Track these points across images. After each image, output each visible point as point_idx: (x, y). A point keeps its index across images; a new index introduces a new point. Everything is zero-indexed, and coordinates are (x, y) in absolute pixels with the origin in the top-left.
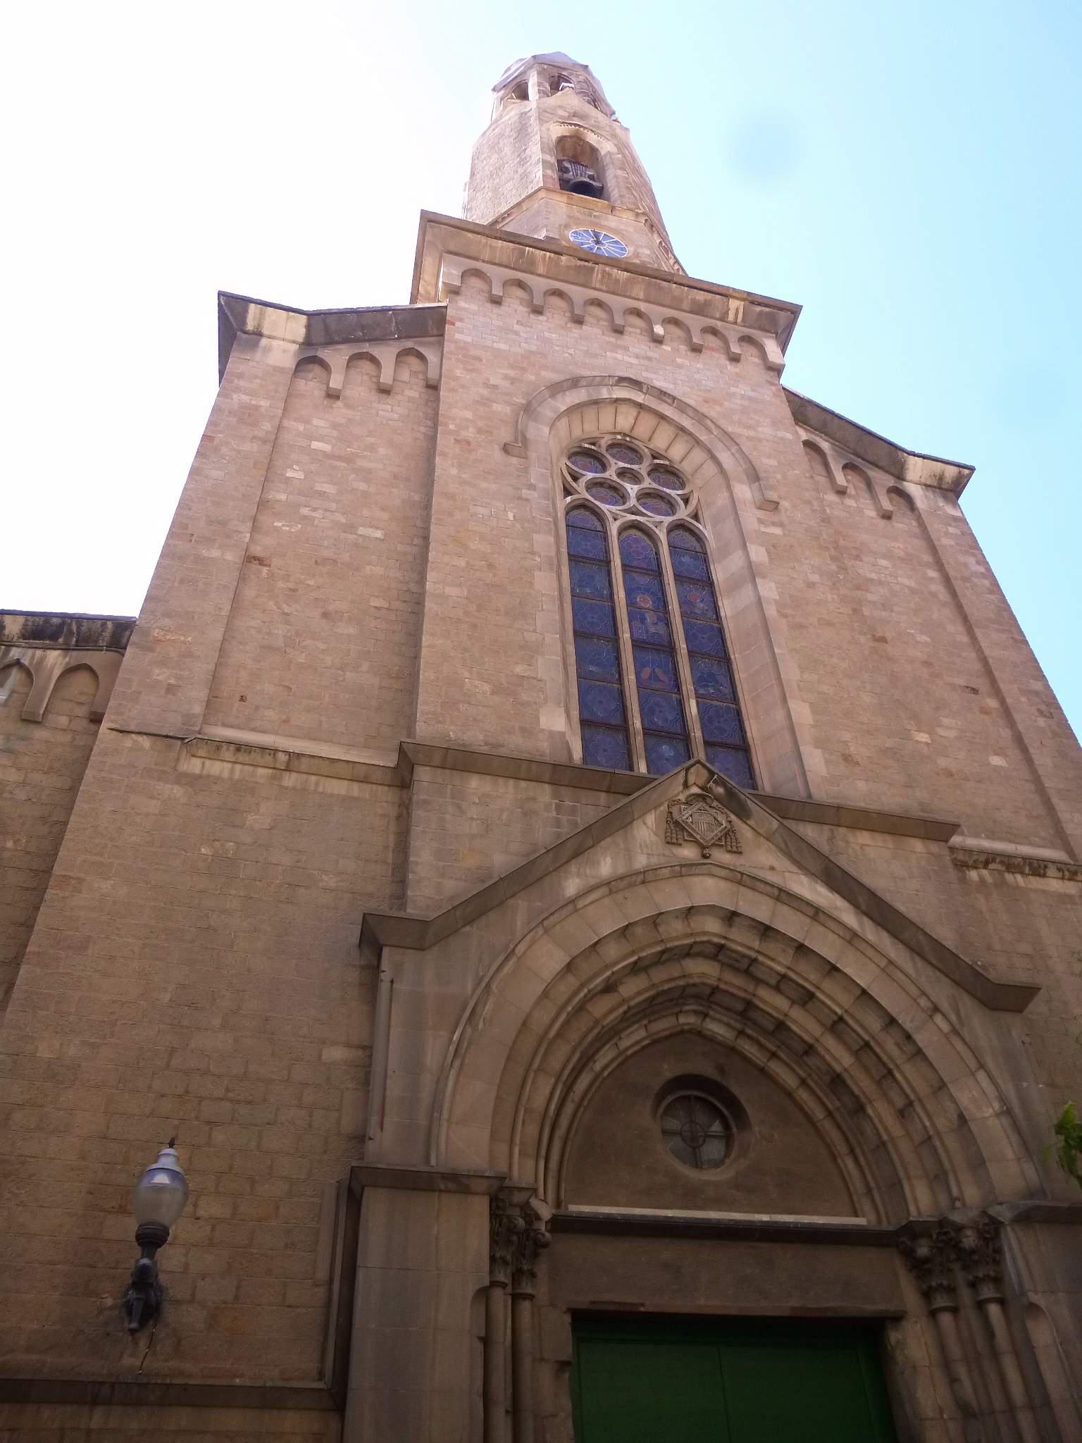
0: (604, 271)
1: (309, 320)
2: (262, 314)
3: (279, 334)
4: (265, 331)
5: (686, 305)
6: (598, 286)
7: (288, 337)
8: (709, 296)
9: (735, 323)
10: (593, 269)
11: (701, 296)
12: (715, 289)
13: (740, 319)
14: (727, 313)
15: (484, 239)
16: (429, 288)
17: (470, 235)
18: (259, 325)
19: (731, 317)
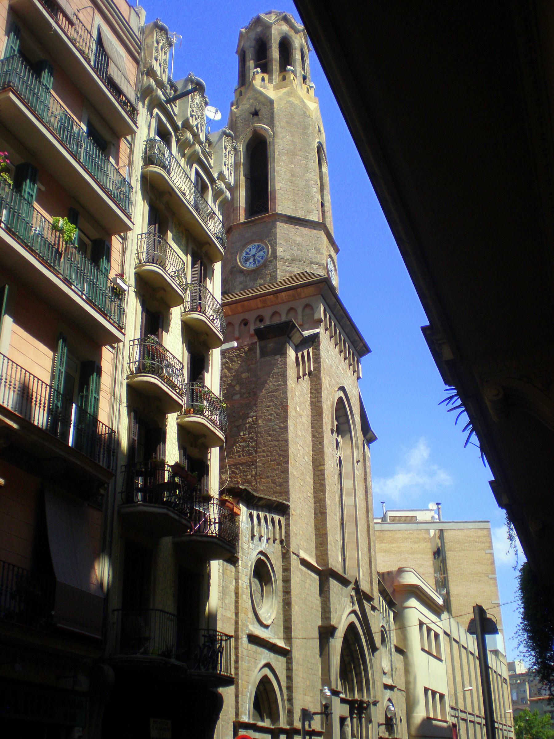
8: (359, 339)
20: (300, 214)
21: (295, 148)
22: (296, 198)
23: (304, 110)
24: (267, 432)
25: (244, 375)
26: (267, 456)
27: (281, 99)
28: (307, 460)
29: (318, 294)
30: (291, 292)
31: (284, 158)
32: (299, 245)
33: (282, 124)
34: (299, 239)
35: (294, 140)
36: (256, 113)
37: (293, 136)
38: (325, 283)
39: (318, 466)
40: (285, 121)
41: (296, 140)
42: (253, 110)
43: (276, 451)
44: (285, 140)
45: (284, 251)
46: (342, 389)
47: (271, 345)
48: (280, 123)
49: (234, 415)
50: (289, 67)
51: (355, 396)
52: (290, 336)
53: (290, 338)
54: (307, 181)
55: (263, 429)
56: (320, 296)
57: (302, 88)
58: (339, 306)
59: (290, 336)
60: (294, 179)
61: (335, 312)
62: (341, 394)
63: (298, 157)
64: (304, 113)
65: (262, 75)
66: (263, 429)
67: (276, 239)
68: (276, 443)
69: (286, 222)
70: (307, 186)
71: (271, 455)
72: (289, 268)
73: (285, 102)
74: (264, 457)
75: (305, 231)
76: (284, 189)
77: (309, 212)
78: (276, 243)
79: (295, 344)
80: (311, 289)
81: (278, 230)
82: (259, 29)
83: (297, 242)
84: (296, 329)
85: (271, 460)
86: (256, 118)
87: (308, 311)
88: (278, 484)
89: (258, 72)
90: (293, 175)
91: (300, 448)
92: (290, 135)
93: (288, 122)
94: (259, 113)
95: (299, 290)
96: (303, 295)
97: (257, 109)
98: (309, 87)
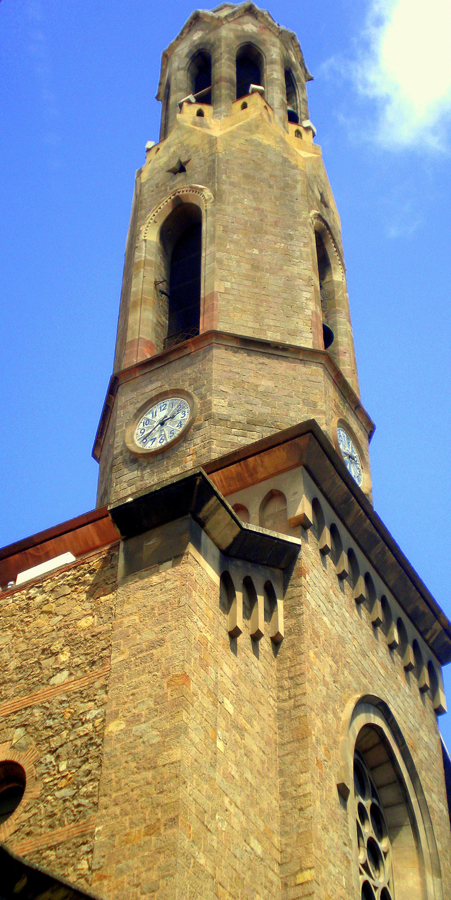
0: (384, 548)
1: (240, 532)
2: (214, 511)
3: (215, 534)
4: (208, 526)
5: (410, 609)
6: (372, 557)
7: (219, 540)
8: (426, 609)
9: (427, 641)
10: (378, 542)
11: (423, 607)
12: (433, 606)
13: (431, 641)
14: (427, 631)
15: (333, 472)
16: (260, 469)
17: (328, 462)
18: (207, 518)
19: (427, 636)
20: (271, 336)
21: (261, 220)
22: (262, 309)
23: (285, 155)
24: (129, 750)
25: (83, 623)
26: (124, 813)
27: (232, 135)
28: (259, 850)
29: (297, 466)
30: (233, 468)
31: (235, 237)
32: (266, 394)
33: (235, 178)
34: (265, 384)
35: (261, 207)
36: (181, 168)
37: (256, 196)
38: (310, 434)
39: (295, 874)
40: (240, 175)
41: (266, 206)
42: (174, 164)
43: (148, 795)
44: (239, 206)
45: (230, 405)
46: (382, 708)
47: (152, 542)
48: (228, 177)
49: (50, 722)
50: (253, 86)
51: (427, 748)
52: (201, 515)
53: (202, 524)
54: (289, 279)
55: (118, 746)
56: (301, 468)
57: (285, 127)
58: (357, 506)
59: (201, 515)
60: (259, 274)
61: (349, 522)
62: (379, 721)
63: (267, 237)
64: (285, 160)
65: (199, 106)
66: (118, 746)
67: (210, 382)
68: (149, 775)
69: (236, 350)
70: (289, 285)
71: (134, 808)
72: (240, 438)
73: (242, 141)
74: (116, 817)
75: (281, 367)
76: (235, 292)
77: (294, 333)
78: (210, 390)
79: (218, 546)
80: (279, 456)
81: (214, 366)
82: (197, 36)
83: (261, 389)
84: (213, 500)
85: (132, 823)
86: (180, 177)
87: (274, 507)
88: (145, 886)
89: (189, 102)
90: (256, 267)
91: (232, 809)
92: (251, 197)
93: (246, 176)
94: (187, 167)
95: (250, 460)
96: (261, 473)
97: (183, 161)
98: (301, 129)
